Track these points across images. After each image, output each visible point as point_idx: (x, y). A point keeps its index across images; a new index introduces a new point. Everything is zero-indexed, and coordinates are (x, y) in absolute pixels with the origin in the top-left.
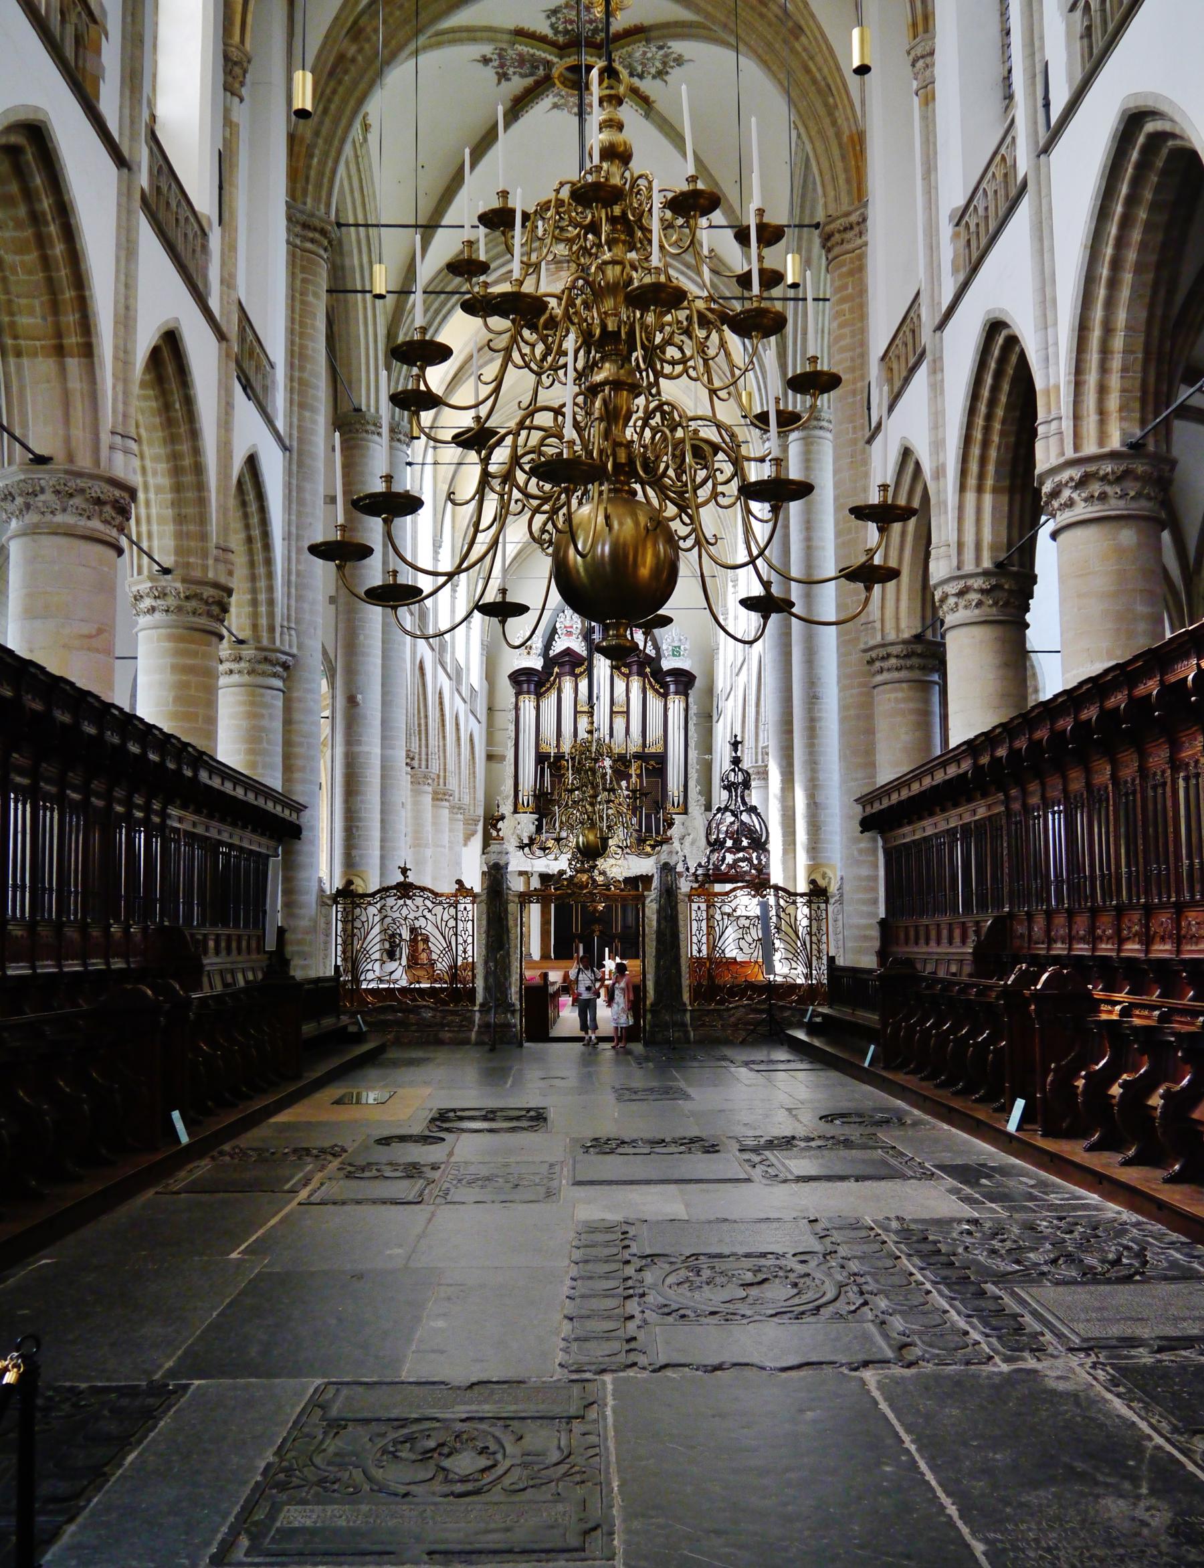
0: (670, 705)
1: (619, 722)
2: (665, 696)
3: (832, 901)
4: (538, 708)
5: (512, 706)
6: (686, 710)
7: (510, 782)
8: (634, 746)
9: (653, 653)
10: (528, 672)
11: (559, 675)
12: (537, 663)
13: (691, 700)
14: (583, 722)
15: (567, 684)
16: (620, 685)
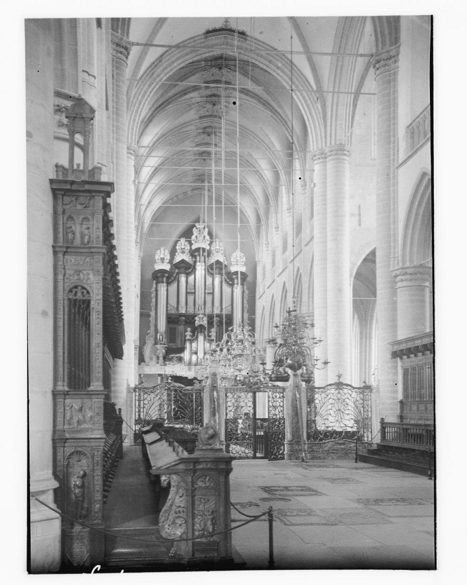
0: (235, 290)
1: (209, 298)
2: (232, 285)
3: (374, 391)
4: (167, 290)
5: (153, 289)
6: (243, 292)
7: (152, 328)
8: (217, 311)
9: (226, 263)
10: (163, 271)
11: (178, 274)
12: (167, 267)
13: (245, 287)
14: (191, 298)
15: (183, 279)
16: (209, 280)
